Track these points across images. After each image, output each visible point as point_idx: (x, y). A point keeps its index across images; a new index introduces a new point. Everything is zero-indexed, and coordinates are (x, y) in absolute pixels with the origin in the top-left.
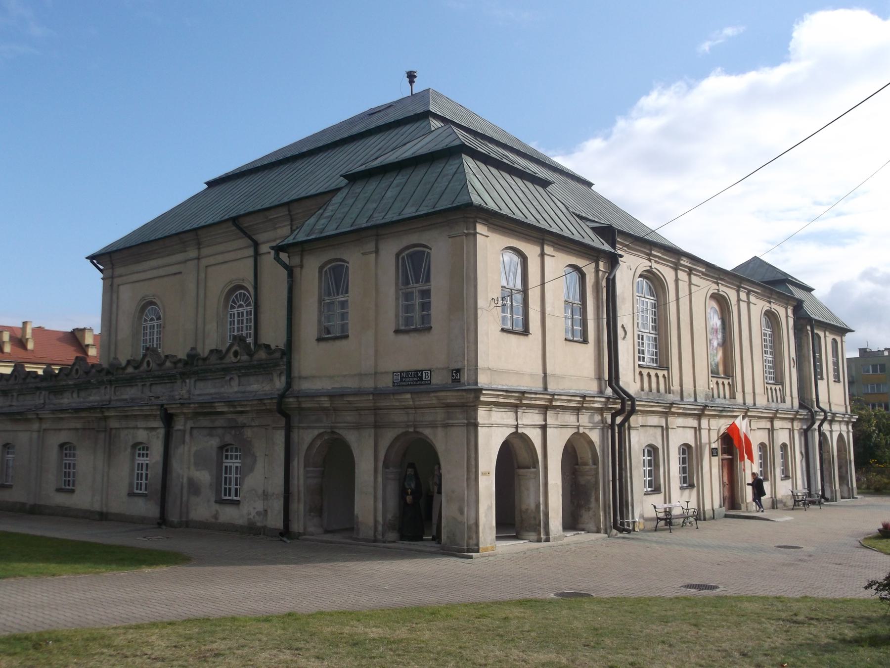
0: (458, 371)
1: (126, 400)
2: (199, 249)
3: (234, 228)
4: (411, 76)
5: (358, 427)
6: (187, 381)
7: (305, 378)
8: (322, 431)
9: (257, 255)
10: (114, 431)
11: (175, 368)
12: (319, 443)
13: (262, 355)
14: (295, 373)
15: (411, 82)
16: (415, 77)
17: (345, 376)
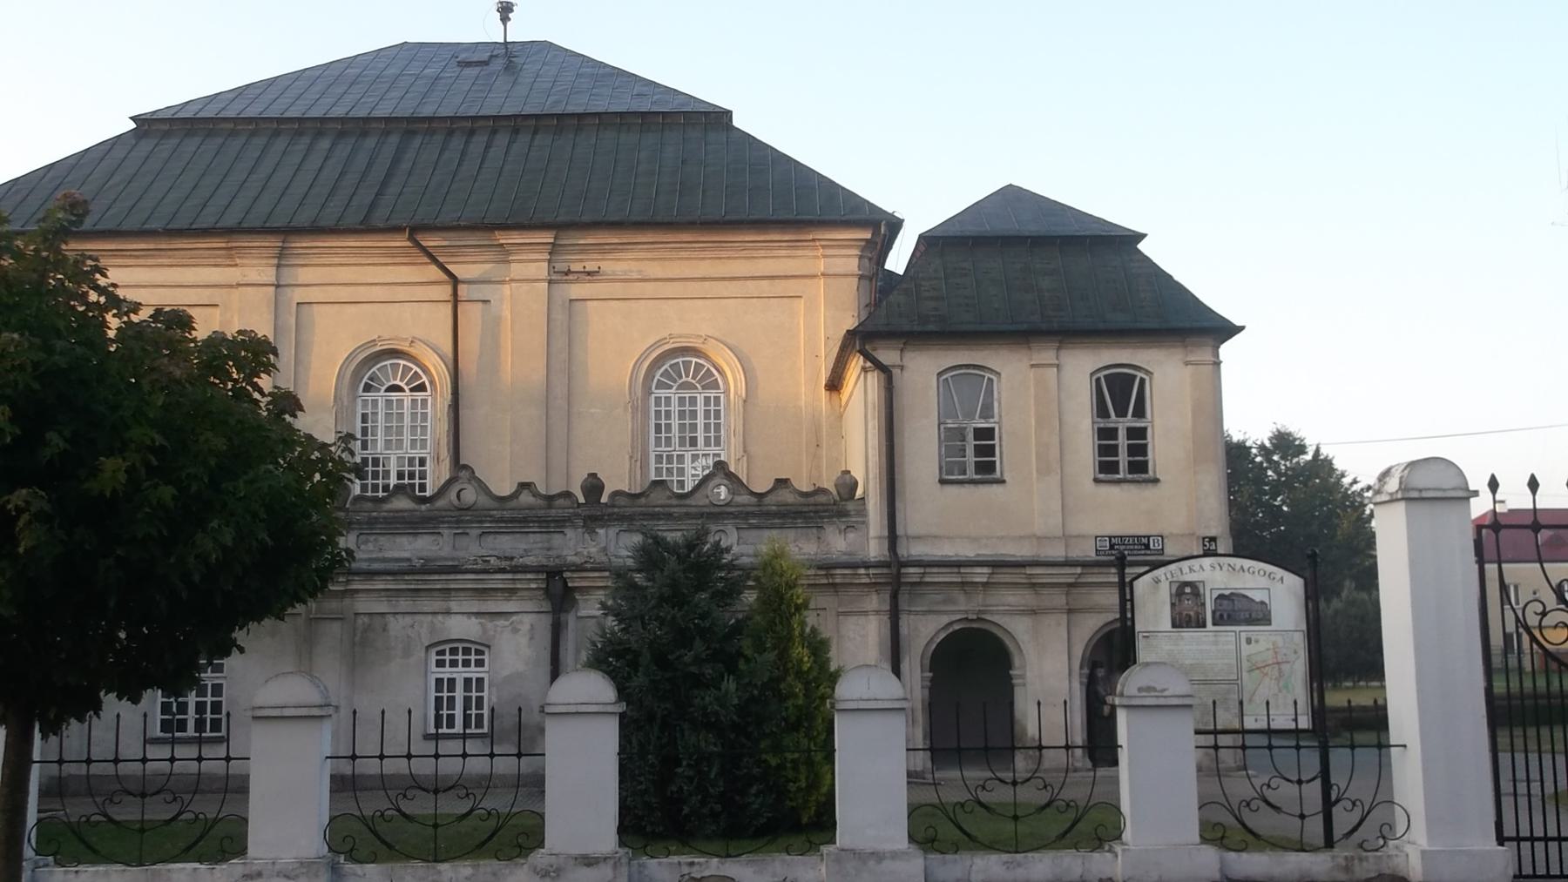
0: (1213, 539)
1: (409, 560)
3: (408, 244)
4: (505, 11)
5: (1033, 612)
6: (601, 531)
7: (919, 538)
8: (959, 617)
9: (456, 301)
10: (361, 621)
11: (550, 507)
12: (942, 636)
13: (787, 497)
14: (900, 531)
17: (1002, 538)
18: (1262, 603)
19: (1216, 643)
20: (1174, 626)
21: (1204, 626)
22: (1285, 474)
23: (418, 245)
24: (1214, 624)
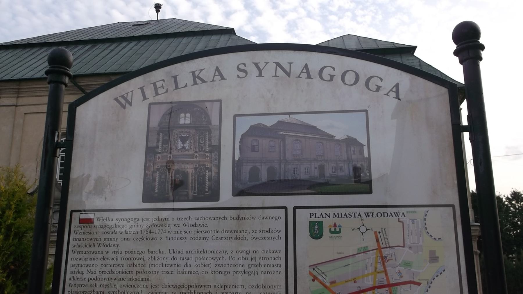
2: (18, 97)
4: (158, 7)
15: (158, 11)
16: (160, 8)
18: (350, 142)
19: (236, 235)
20: (147, 197)
21: (215, 196)
22: (518, 209)
23: (76, 85)
24: (238, 192)
